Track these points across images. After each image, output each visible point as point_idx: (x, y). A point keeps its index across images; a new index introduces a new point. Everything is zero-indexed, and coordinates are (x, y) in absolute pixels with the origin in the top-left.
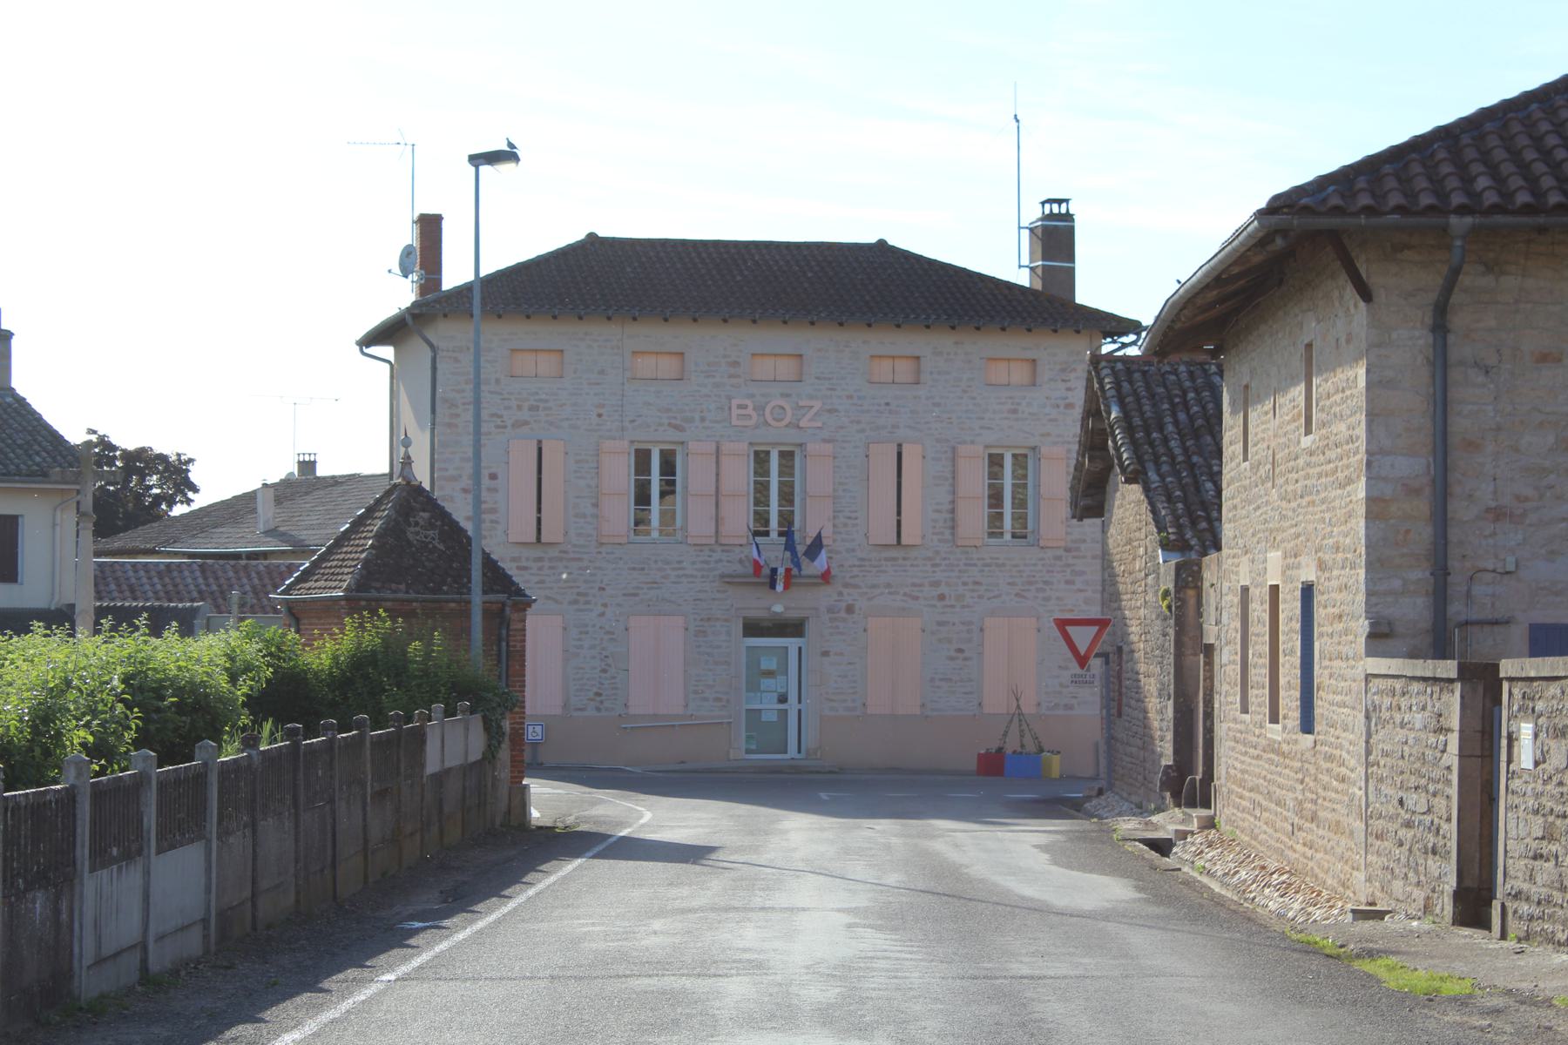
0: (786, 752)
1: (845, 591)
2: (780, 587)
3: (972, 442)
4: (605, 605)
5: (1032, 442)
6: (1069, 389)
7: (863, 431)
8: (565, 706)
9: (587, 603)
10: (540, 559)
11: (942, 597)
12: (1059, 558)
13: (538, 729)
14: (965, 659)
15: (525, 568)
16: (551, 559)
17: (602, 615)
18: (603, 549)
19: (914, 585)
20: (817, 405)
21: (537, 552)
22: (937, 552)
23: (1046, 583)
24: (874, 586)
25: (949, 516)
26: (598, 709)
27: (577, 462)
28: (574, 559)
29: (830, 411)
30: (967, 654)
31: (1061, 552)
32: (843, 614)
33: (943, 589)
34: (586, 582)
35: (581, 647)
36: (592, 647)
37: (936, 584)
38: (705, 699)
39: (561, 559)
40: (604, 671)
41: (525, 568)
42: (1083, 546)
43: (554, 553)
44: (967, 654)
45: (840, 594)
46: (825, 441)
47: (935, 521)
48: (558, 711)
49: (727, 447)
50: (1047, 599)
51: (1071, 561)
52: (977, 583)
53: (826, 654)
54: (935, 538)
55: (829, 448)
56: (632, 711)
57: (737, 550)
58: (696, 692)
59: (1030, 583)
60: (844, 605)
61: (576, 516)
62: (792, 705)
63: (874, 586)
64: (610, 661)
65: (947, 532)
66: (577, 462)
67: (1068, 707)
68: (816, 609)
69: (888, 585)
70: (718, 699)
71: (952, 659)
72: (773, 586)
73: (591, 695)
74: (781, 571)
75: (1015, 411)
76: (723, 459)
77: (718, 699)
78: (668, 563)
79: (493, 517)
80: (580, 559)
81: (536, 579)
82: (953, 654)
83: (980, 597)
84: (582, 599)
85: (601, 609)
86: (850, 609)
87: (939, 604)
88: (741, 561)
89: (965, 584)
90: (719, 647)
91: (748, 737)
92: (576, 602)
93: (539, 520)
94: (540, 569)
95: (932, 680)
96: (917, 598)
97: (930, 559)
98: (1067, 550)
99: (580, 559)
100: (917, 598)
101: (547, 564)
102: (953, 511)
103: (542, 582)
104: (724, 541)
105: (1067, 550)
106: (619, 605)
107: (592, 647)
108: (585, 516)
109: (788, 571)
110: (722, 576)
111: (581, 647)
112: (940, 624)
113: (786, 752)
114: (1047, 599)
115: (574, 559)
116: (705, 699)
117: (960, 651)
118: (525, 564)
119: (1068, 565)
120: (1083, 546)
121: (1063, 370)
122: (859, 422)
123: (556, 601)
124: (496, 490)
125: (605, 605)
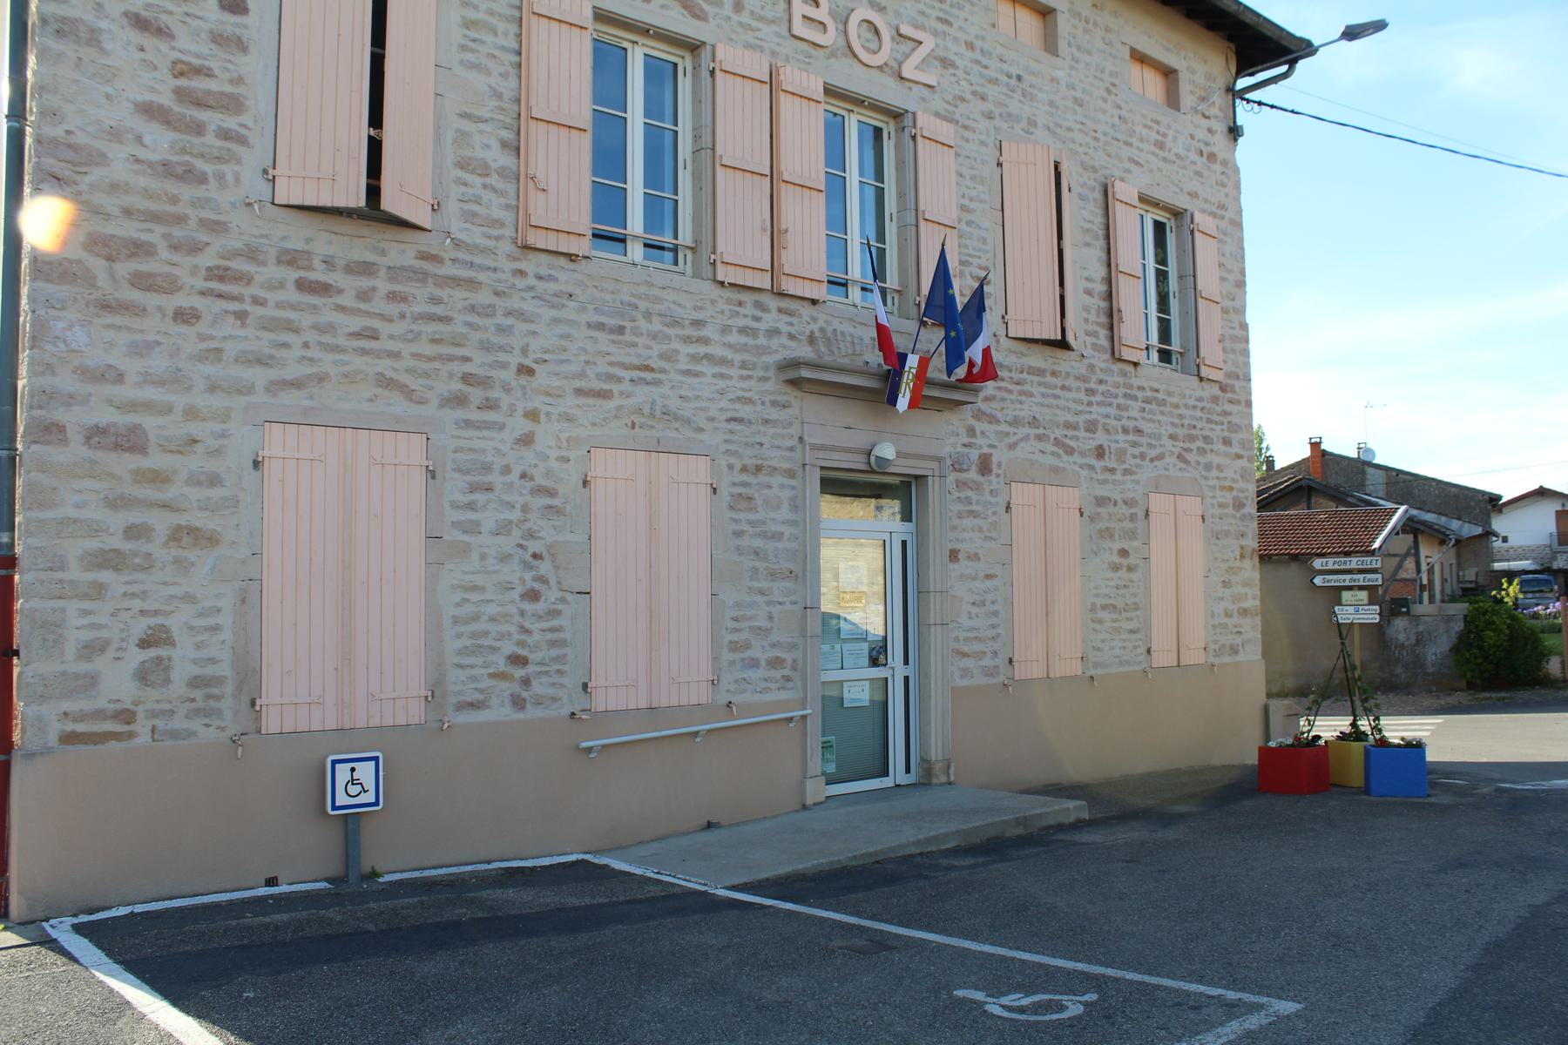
0: (885, 773)
1: (980, 427)
2: (903, 403)
3: (1122, 180)
4: (533, 415)
5: (1181, 202)
6: (1210, 130)
7: (990, 117)
8: (434, 696)
9: (490, 405)
10: (366, 269)
11: (1100, 452)
12: (1215, 399)
13: (365, 772)
14: (1130, 569)
15: (324, 289)
16: (394, 273)
17: (526, 440)
18: (531, 264)
19: (1068, 425)
20: (929, 43)
21: (358, 244)
22: (1091, 367)
23: (1207, 439)
24: (1016, 422)
25: (1104, 304)
26: (518, 703)
27: (468, 24)
28: (456, 282)
29: (946, 63)
30: (1132, 560)
31: (1216, 390)
32: (973, 475)
33: (1101, 438)
34: (486, 347)
35: (472, 528)
36: (503, 529)
37: (1091, 427)
38: (754, 663)
39: (423, 277)
40: (532, 596)
41: (324, 289)
42: (1238, 384)
43: (400, 251)
44: (1132, 560)
45: (971, 432)
46: (937, 114)
47: (1087, 309)
48: (415, 713)
49: (791, 77)
50: (1208, 467)
51: (1228, 407)
52: (1139, 431)
53: (954, 555)
54: (1090, 340)
55: (946, 131)
56: (600, 702)
57: (806, 311)
58: (734, 647)
59: (1192, 438)
60: (974, 455)
61: (462, 164)
62: (896, 668)
63: (1016, 422)
64: (545, 567)
65: (1103, 333)
66: (468, 24)
67: (1234, 650)
68: (939, 460)
69: (1034, 422)
70: (776, 663)
71: (1116, 568)
72: (893, 401)
73: (501, 664)
74: (912, 361)
75: (1160, 145)
76: (786, 104)
77: (776, 663)
78: (676, 323)
79: (231, 123)
80: (472, 284)
81: (356, 323)
82: (1116, 559)
83: (1142, 456)
84: (476, 395)
85: (521, 425)
86: (985, 466)
87: (1098, 464)
88: (812, 340)
89: (1125, 431)
90: (778, 536)
91: (826, 747)
92: (460, 400)
93: (375, 148)
94: (364, 296)
95: (1093, 609)
96: (1070, 451)
97: (1084, 379)
98: (1223, 388)
99: (472, 284)
100: (1070, 451)
101: (383, 285)
102: (1109, 296)
103: (374, 336)
104: (790, 286)
105: (1223, 388)
106: (569, 419)
107: (503, 529)
108: (484, 170)
109: (924, 363)
110: (795, 364)
111: (472, 528)
112: (1101, 501)
113: (885, 773)
114: (1208, 467)
115: (456, 282)
116: (754, 663)
117: (1124, 553)
118: (318, 275)
119: (1225, 413)
120: (1238, 384)
121: (1202, 99)
122: (983, 98)
123: (408, 393)
124: (240, 45)
125: (533, 415)
